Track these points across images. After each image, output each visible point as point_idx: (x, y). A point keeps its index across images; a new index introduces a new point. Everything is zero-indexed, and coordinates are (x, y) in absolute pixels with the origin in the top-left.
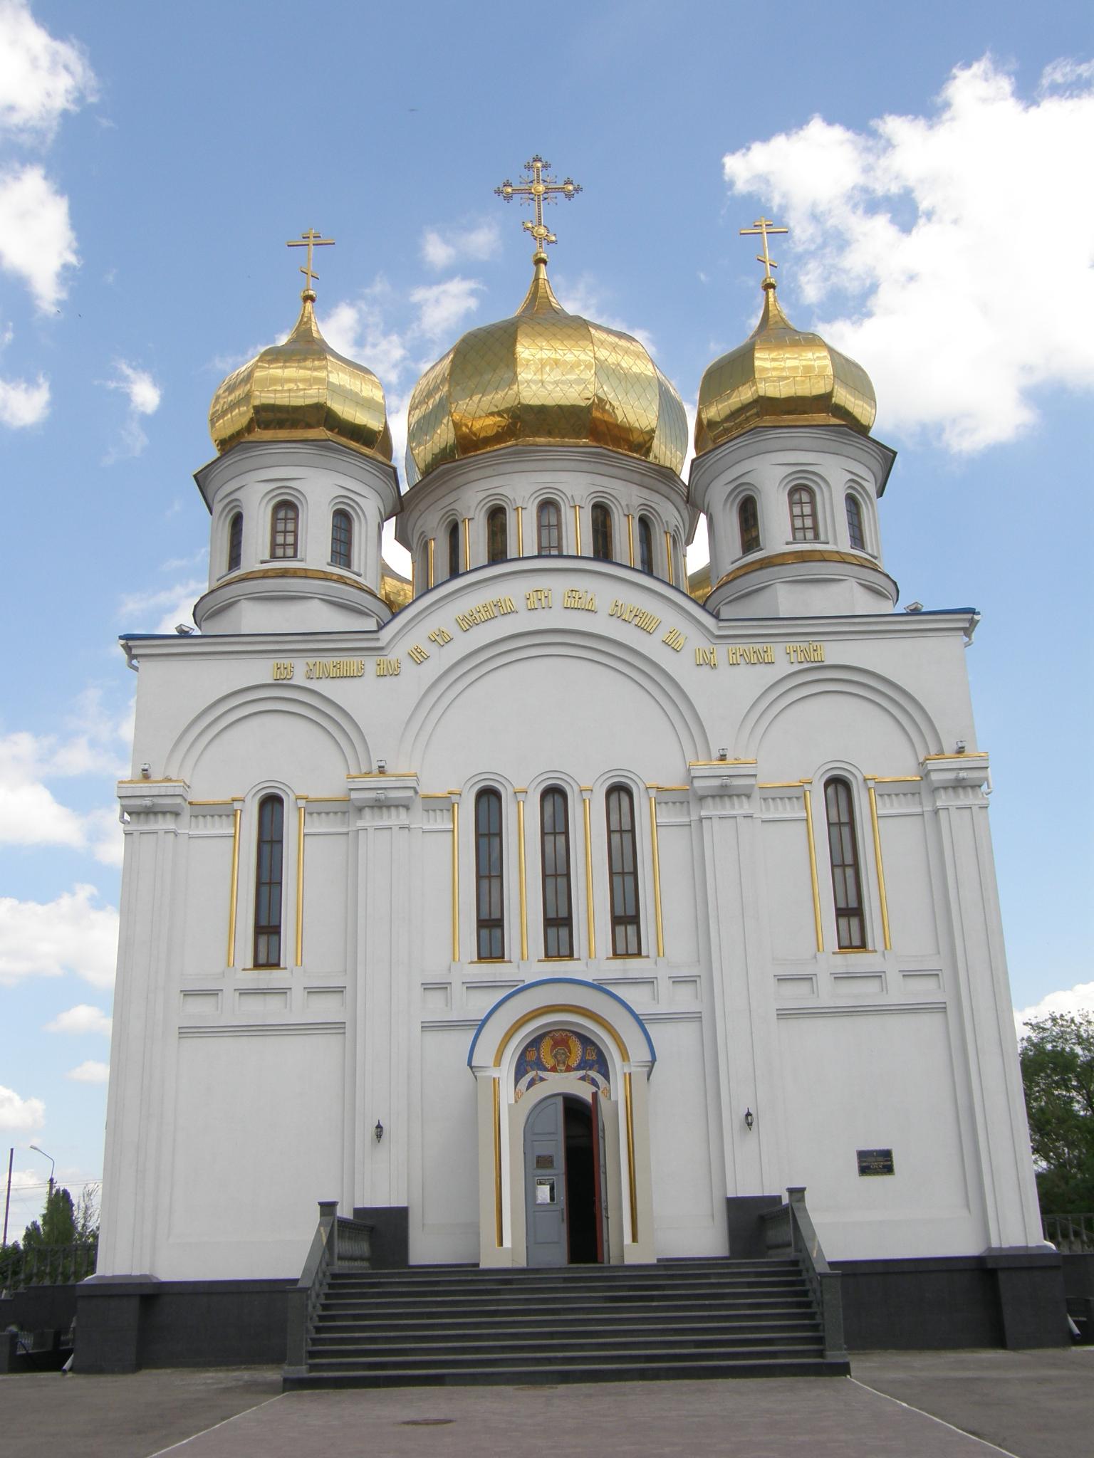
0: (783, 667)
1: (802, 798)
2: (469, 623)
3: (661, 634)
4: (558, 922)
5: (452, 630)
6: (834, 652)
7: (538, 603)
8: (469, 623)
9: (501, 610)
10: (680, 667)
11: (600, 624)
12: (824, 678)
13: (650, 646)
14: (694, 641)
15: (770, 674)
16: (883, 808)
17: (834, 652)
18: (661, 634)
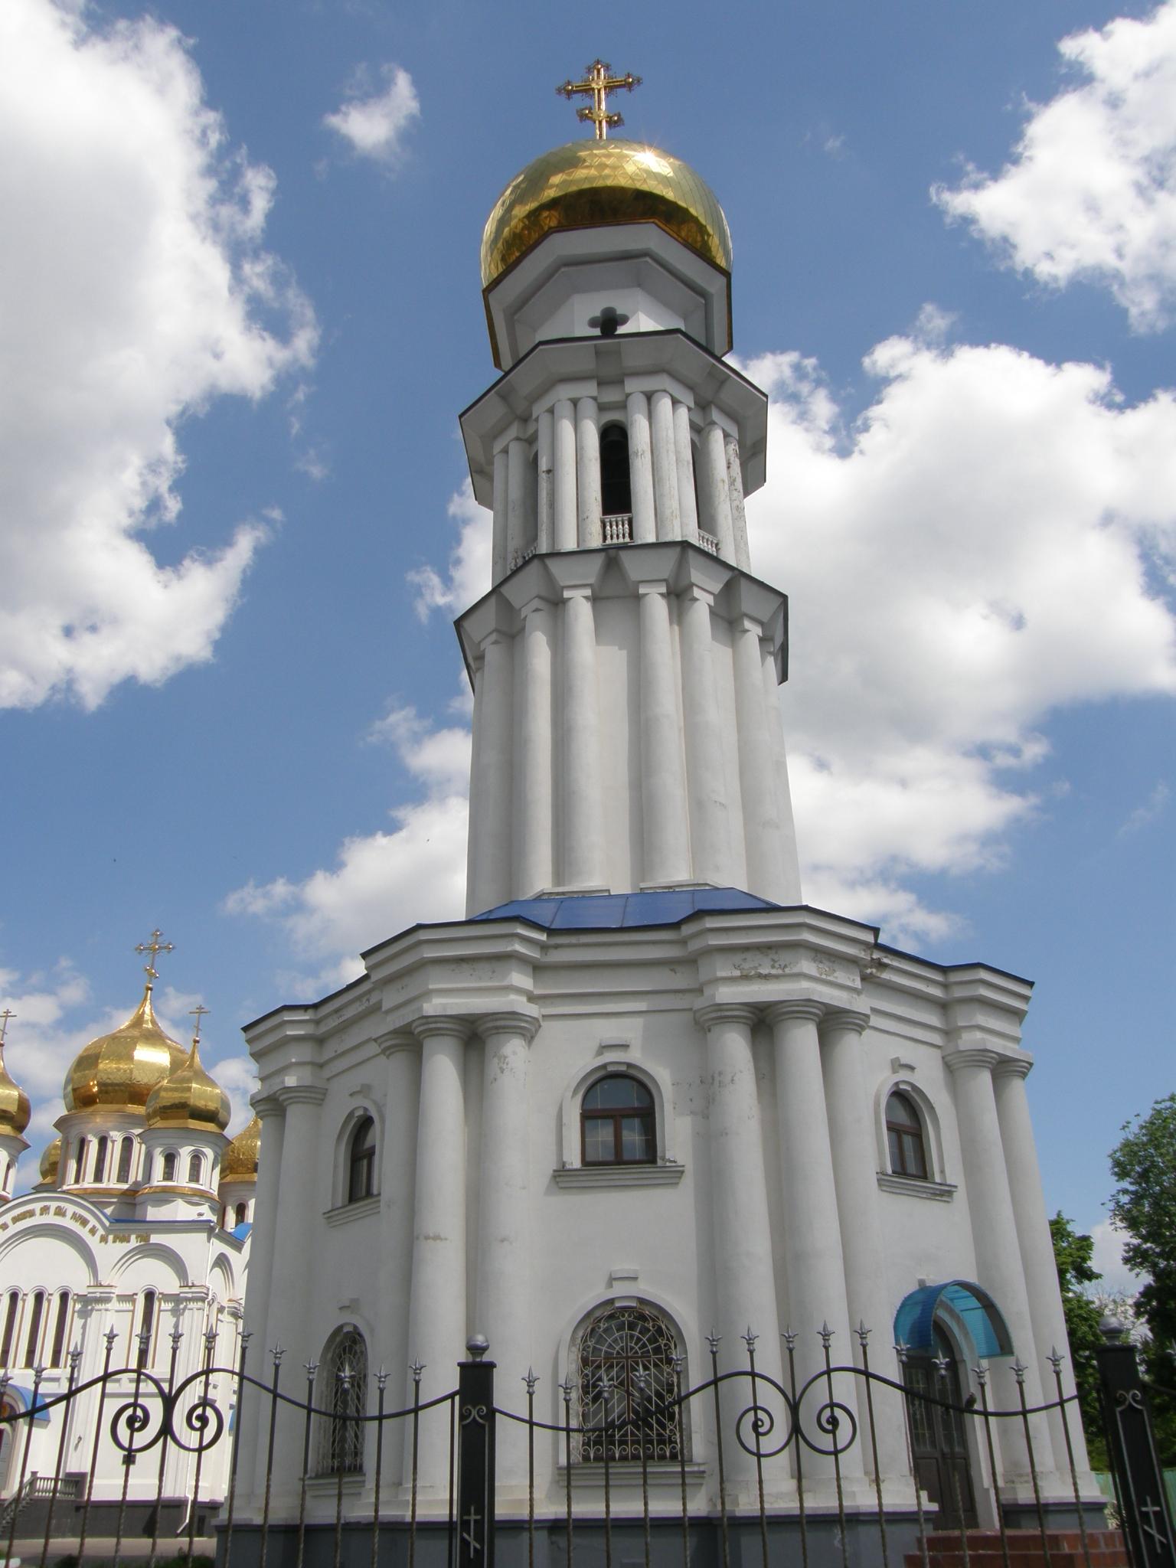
0: (134, 1242)
1: (134, 1302)
2: (15, 1220)
3: (89, 1226)
4: (31, 1352)
5: (10, 1223)
6: (155, 1239)
7: (45, 1210)
8: (15, 1220)
9: (31, 1214)
10: (93, 1242)
11: (67, 1222)
12: (149, 1250)
13: (83, 1232)
14: (101, 1232)
15: (126, 1247)
16: (164, 1306)
17: (155, 1239)
18: (89, 1226)
